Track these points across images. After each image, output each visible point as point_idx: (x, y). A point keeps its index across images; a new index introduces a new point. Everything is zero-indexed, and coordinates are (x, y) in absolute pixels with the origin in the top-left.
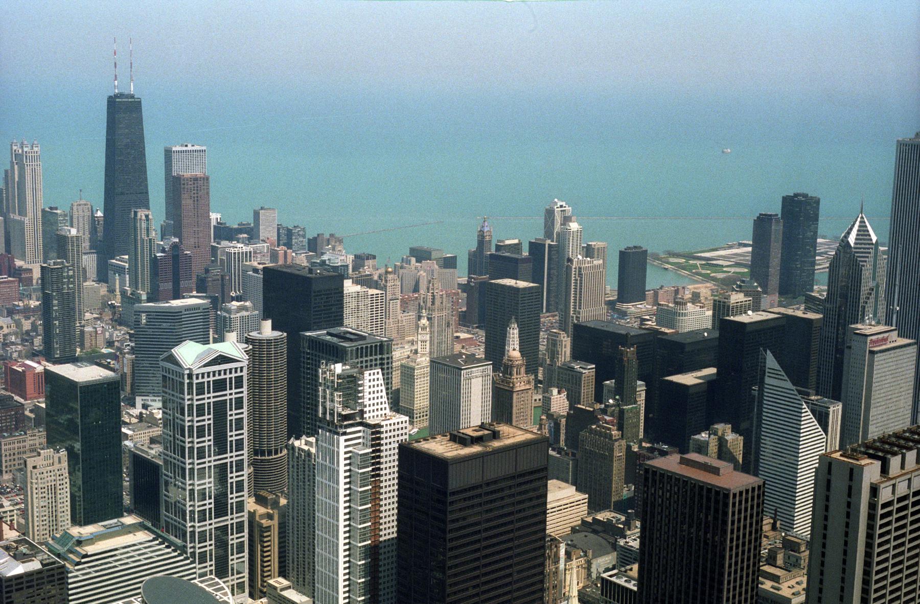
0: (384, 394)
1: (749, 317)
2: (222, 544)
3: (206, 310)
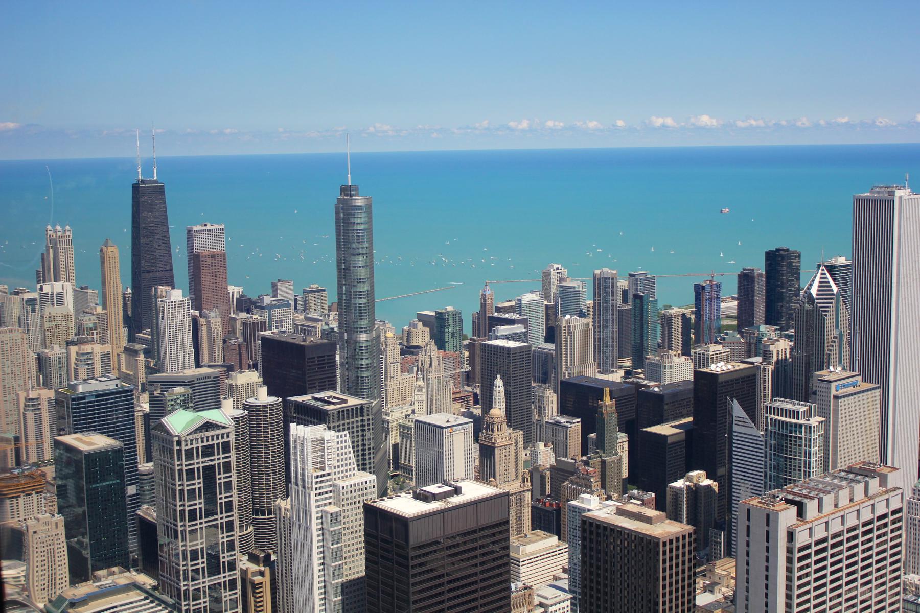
0: (352, 455)
1: (718, 368)
3: (217, 380)
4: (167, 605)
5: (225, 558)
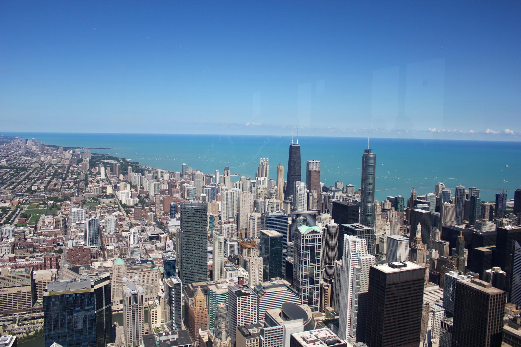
0: (366, 248)
1: (508, 227)
2: (311, 293)
4: (295, 293)
5: (316, 279)
